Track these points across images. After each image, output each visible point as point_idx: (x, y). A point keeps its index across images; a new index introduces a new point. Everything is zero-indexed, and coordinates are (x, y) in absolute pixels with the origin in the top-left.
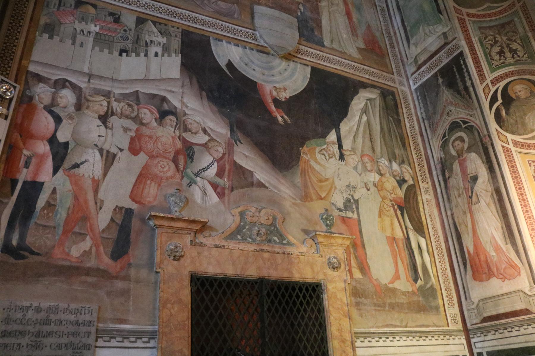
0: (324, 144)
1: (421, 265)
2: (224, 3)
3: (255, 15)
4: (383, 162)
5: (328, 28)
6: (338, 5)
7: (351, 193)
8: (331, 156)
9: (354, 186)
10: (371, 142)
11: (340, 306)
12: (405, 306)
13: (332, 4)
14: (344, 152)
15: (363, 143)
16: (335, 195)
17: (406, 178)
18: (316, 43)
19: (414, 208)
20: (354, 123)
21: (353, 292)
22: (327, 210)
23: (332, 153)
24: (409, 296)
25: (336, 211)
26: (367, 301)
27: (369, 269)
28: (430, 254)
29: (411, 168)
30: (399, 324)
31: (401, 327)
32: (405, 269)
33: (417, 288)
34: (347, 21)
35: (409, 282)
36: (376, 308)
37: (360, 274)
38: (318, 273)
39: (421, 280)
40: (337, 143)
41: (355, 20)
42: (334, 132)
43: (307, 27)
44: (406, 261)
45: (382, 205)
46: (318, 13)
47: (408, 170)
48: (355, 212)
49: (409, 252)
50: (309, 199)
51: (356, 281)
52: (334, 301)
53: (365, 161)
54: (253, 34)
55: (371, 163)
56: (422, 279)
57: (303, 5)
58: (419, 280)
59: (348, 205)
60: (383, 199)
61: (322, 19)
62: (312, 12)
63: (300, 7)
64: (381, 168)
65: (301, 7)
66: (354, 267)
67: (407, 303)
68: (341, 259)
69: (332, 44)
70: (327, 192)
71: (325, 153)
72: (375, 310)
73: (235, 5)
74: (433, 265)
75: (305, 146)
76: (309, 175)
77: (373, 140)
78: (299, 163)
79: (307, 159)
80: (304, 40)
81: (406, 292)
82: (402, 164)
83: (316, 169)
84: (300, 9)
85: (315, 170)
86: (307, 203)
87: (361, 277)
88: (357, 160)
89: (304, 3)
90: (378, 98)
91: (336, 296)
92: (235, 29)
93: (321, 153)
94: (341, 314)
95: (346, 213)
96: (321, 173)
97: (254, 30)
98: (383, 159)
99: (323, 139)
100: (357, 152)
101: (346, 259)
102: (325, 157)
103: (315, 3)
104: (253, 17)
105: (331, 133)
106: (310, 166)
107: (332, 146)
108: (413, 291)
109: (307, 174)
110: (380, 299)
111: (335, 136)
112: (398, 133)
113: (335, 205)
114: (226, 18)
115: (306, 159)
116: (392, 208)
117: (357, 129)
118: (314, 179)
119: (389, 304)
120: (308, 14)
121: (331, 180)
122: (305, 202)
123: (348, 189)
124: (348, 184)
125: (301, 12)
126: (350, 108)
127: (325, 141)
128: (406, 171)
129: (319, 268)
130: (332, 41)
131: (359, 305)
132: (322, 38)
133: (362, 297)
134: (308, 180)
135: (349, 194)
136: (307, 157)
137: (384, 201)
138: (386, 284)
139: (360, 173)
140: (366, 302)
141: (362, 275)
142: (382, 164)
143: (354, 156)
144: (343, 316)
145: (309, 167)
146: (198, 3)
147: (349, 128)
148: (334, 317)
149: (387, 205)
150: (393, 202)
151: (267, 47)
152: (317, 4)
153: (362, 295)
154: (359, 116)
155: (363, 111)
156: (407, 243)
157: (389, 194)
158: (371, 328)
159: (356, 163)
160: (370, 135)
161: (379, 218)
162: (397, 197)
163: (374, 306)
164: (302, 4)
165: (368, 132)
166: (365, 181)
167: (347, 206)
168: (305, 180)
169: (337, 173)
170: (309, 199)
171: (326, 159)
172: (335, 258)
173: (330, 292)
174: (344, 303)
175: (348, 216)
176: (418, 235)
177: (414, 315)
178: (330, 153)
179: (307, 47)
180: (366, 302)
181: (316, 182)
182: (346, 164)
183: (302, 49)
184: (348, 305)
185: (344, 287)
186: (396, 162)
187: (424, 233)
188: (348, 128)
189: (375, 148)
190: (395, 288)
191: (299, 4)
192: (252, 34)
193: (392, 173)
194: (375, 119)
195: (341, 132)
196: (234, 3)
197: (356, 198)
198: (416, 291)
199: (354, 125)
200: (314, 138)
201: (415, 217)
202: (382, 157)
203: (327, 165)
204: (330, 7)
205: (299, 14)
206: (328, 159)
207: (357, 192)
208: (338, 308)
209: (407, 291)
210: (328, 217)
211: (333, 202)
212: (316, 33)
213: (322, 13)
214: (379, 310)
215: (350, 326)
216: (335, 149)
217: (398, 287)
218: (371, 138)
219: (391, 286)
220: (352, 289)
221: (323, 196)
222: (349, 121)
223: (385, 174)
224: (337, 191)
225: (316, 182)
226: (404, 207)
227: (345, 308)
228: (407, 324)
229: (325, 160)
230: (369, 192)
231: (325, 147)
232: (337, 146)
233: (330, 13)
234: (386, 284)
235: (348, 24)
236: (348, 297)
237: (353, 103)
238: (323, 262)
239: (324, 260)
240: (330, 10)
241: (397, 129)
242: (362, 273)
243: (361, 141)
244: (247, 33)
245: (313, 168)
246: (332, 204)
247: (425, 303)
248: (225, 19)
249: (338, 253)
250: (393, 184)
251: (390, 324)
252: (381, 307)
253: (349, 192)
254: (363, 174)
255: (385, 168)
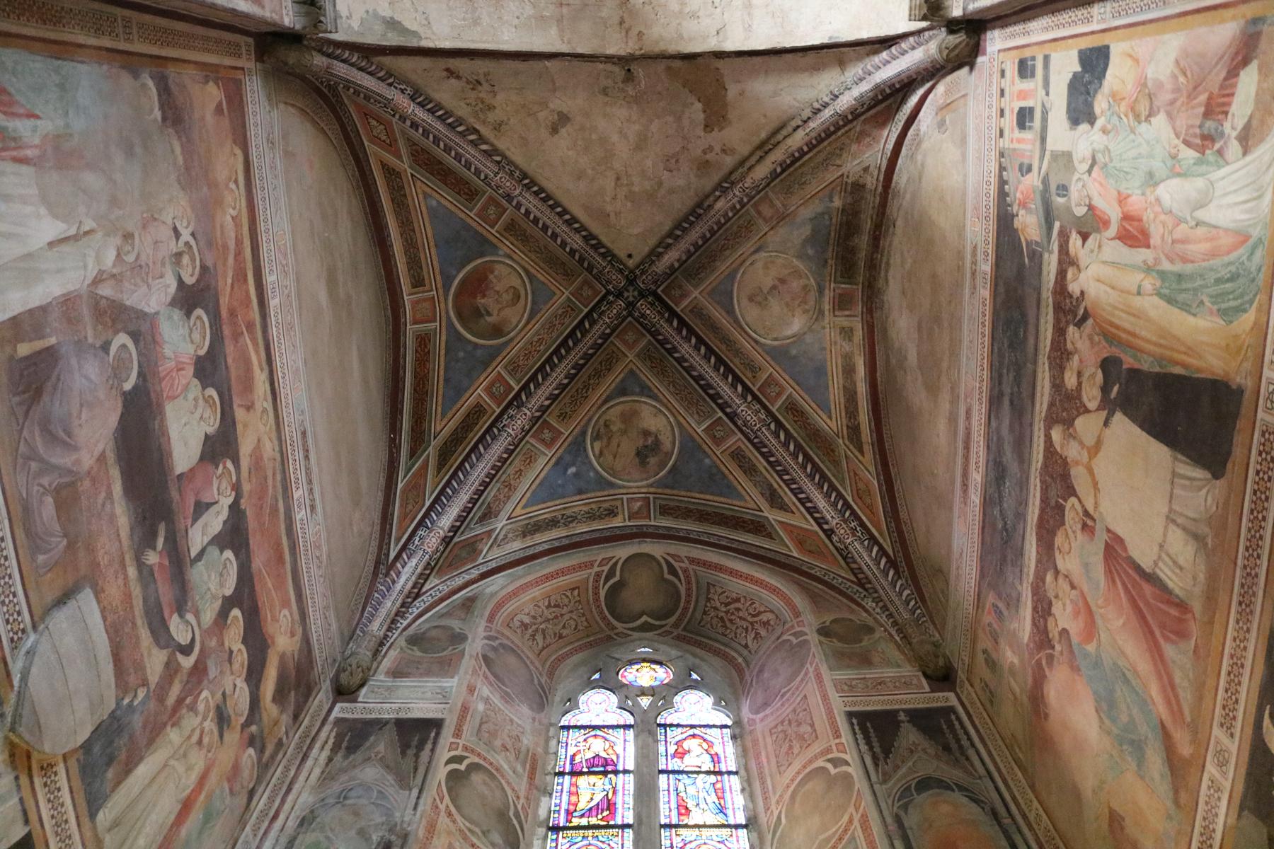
2: (54, 512)
3: (72, 604)
5: (136, 790)
6: (189, 769)
13: (185, 756)
18: (90, 793)
34: (172, 817)
41: (184, 832)
43: (112, 742)
46: (151, 742)
54: (23, 631)
57: (147, 696)
61: (145, 761)
62: (144, 727)
63: (139, 691)
65: (141, 693)
69: (109, 830)
73: (65, 542)
80: (78, 760)
84: (135, 696)
89: (151, 694)
92: (10, 576)
97: (34, 627)
103: (165, 718)
104: (61, 601)
114: (23, 536)
120: (137, 721)
125: (132, 701)
130: (116, 824)
132: (106, 798)
146: (22, 448)
151: (12, 686)
152: (165, 725)
164: (148, 689)
179: (69, 780)
183: (56, 774)
191: (143, 685)
192: (22, 626)
196: (65, 535)
204: (177, 756)
205: (126, 701)
212: (110, 774)
213: (155, 751)
233: (165, 766)
235: (168, 827)
240: (172, 762)
244: (19, 613)
248: (20, 534)
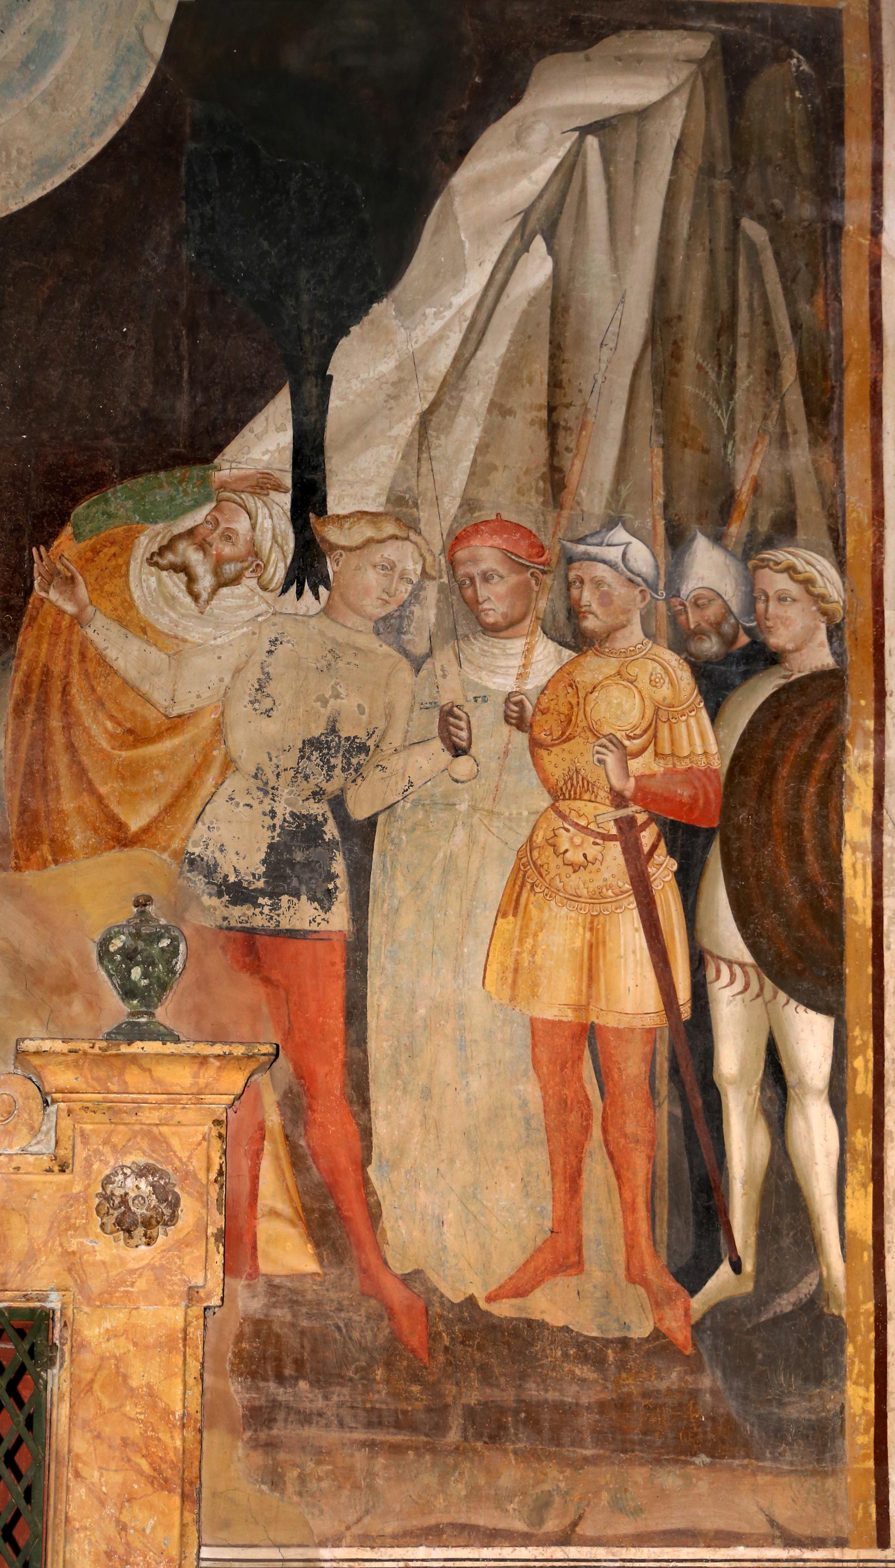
0: (197, 504)
1: (759, 1178)
4: (614, 554)
7: (332, 787)
8: (230, 569)
9: (362, 735)
10: (553, 428)
11: (135, 1432)
12: (586, 1420)
14: (333, 534)
15: (482, 449)
16: (219, 806)
17: (779, 639)
19: (795, 828)
20: (439, 324)
21: (238, 1354)
22: (142, 902)
23: (241, 548)
24: (622, 1365)
25: (215, 901)
26: (326, 1398)
27: (374, 1215)
28: (850, 1110)
29: (841, 565)
30: (520, 1526)
31: (526, 1539)
32: (629, 1208)
33: (695, 1317)
35: (645, 1283)
36: (380, 1436)
37: (310, 1248)
38: (32, 1255)
39: (737, 1267)
40: (288, 481)
42: (282, 404)
44: (651, 1159)
45: (539, 839)
47: (807, 583)
48: (342, 896)
49: (684, 1099)
50: (45, 848)
51: (273, 1288)
52: (106, 1403)
53: (475, 571)
55: (513, 579)
56: (748, 1266)
58: (725, 1269)
59: (299, 856)
60: (557, 794)
64: (587, 596)
66: (274, 1213)
67: (602, 1407)
68: (187, 1176)
70: (165, 798)
71: (195, 557)
72: (371, 1445)
74: (858, 1174)
75: (69, 530)
76: (67, 709)
77: (568, 416)
78: (13, 643)
79: (70, 608)
81: (607, 1342)
82: (769, 543)
83: (120, 664)
85: (109, 669)
86: (30, 877)
87: (312, 1266)
88: (413, 568)
90: (679, 103)
91: (125, 1377)
93: (170, 557)
94: (141, 1473)
95: (275, 907)
96: (145, 688)
98: (620, 535)
99: (196, 471)
100: (424, 514)
101: (213, 1175)
102: (191, 580)
105: (258, 423)
106: (83, 656)
107: (251, 502)
108: (657, 1334)
109: (56, 698)
110: (415, 1389)
111: (286, 438)
112: (796, 326)
113: (210, 871)
115: (61, 612)
116: (615, 850)
117: (456, 359)
118: (95, 730)
119: (470, 1414)
121: (207, 721)
122: (18, 868)
123: (313, 764)
124: (317, 730)
126: (431, 221)
127: (204, 481)
128: (794, 589)
129: (40, 1233)
131: (270, 1422)
133: (300, 1374)
134: (59, 739)
135: (317, 795)
136: (73, 597)
137: (563, 806)
138: (471, 1301)
139: (420, 647)
140: (320, 1403)
141: (320, 1260)
142: (601, 571)
143: (390, 551)
144: (151, 1481)
145: (75, 658)
147: (399, 367)
148: (90, 1490)
149: (585, 829)
150: (632, 809)
153: (299, 1364)
154: (489, 267)
155: (533, 223)
156: (683, 1049)
157: (611, 759)
158: (322, 1544)
159: (404, 591)
160: (555, 383)
161: (502, 913)
162: (671, 773)
163: (369, 1425)
165: (540, 368)
166: (445, 699)
167: (292, 864)
168: (43, 739)
169: (253, 674)
170: (45, 848)
171: (196, 597)
172: (142, 1172)
173: (87, 1358)
174: (168, 1412)
175: (285, 925)
176: (782, 996)
177: (639, 1474)
178: (227, 550)
180: (320, 1403)
181: (105, 744)
182: (326, 611)
184: (183, 1426)
185: (181, 1324)
186: (718, 539)
187: (837, 980)
188: (386, 367)
189: (574, 468)
190: (529, 1323)
193: (673, 619)
194: (616, 265)
195: (334, 402)
197: (359, 811)
198: (681, 1334)
199: (440, 338)
200: (130, 471)
201: (790, 884)
202: (611, 523)
203: (196, 633)
206: (205, 596)
207: (375, 775)
208: (125, 1442)
209: (615, 1333)
210: (141, 945)
211: (197, 851)
214: (396, 1449)
215: (182, 1536)
216: (265, 523)
217: (556, 1317)
218: (551, 409)
219: (504, 1309)
220: (240, 1338)
221: (135, 824)
222: (405, 313)
223: (609, 634)
224: (234, 783)
225: (105, 744)
226: (710, 833)
227: (165, 1437)
228: (575, 1524)
229: (188, 600)
230: (463, 766)
231: (198, 517)
232: (285, 500)
234: (471, 1301)
236: (191, 1381)
237: (461, 179)
238: (72, 1199)
239: (77, 1189)
241: (791, 302)
242: (317, 1245)
243: (476, 433)
245: (102, 660)
246: (193, 862)
247: (732, 1406)
249: (175, 1143)
250: (665, 691)
251: (453, 1525)
252: (413, 1428)
253: (318, 779)
254: (444, 657)
255: (620, 591)
